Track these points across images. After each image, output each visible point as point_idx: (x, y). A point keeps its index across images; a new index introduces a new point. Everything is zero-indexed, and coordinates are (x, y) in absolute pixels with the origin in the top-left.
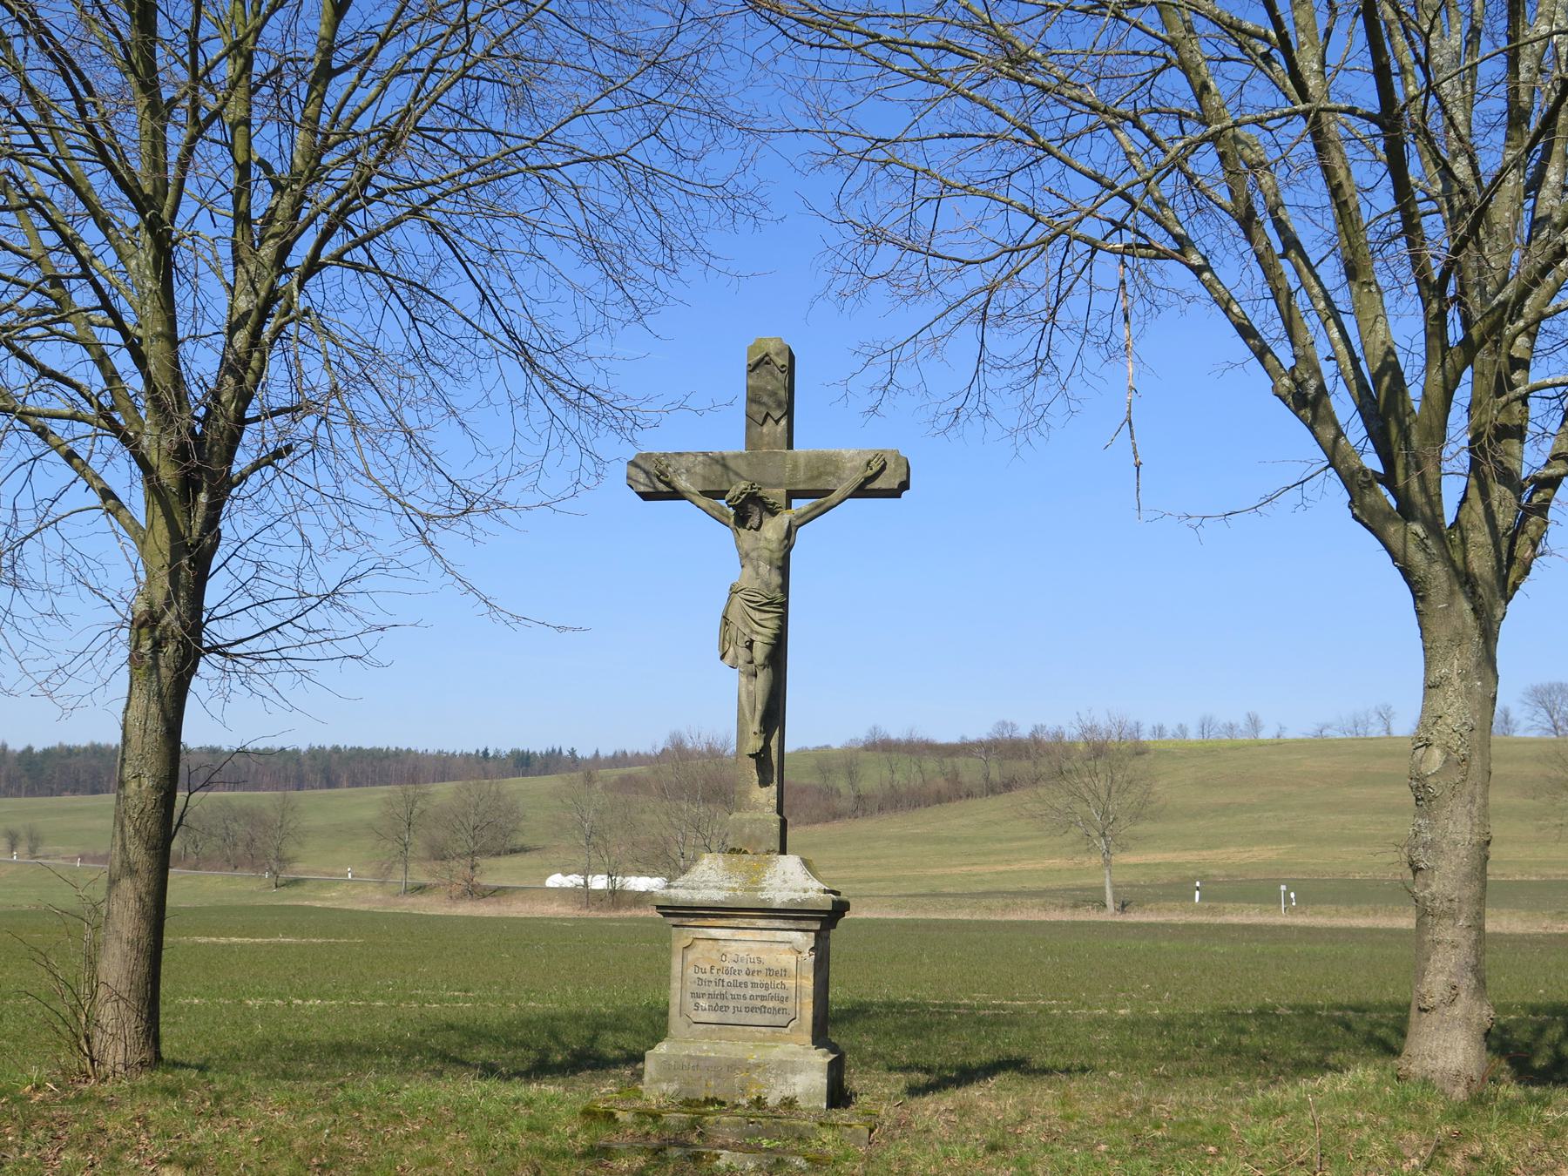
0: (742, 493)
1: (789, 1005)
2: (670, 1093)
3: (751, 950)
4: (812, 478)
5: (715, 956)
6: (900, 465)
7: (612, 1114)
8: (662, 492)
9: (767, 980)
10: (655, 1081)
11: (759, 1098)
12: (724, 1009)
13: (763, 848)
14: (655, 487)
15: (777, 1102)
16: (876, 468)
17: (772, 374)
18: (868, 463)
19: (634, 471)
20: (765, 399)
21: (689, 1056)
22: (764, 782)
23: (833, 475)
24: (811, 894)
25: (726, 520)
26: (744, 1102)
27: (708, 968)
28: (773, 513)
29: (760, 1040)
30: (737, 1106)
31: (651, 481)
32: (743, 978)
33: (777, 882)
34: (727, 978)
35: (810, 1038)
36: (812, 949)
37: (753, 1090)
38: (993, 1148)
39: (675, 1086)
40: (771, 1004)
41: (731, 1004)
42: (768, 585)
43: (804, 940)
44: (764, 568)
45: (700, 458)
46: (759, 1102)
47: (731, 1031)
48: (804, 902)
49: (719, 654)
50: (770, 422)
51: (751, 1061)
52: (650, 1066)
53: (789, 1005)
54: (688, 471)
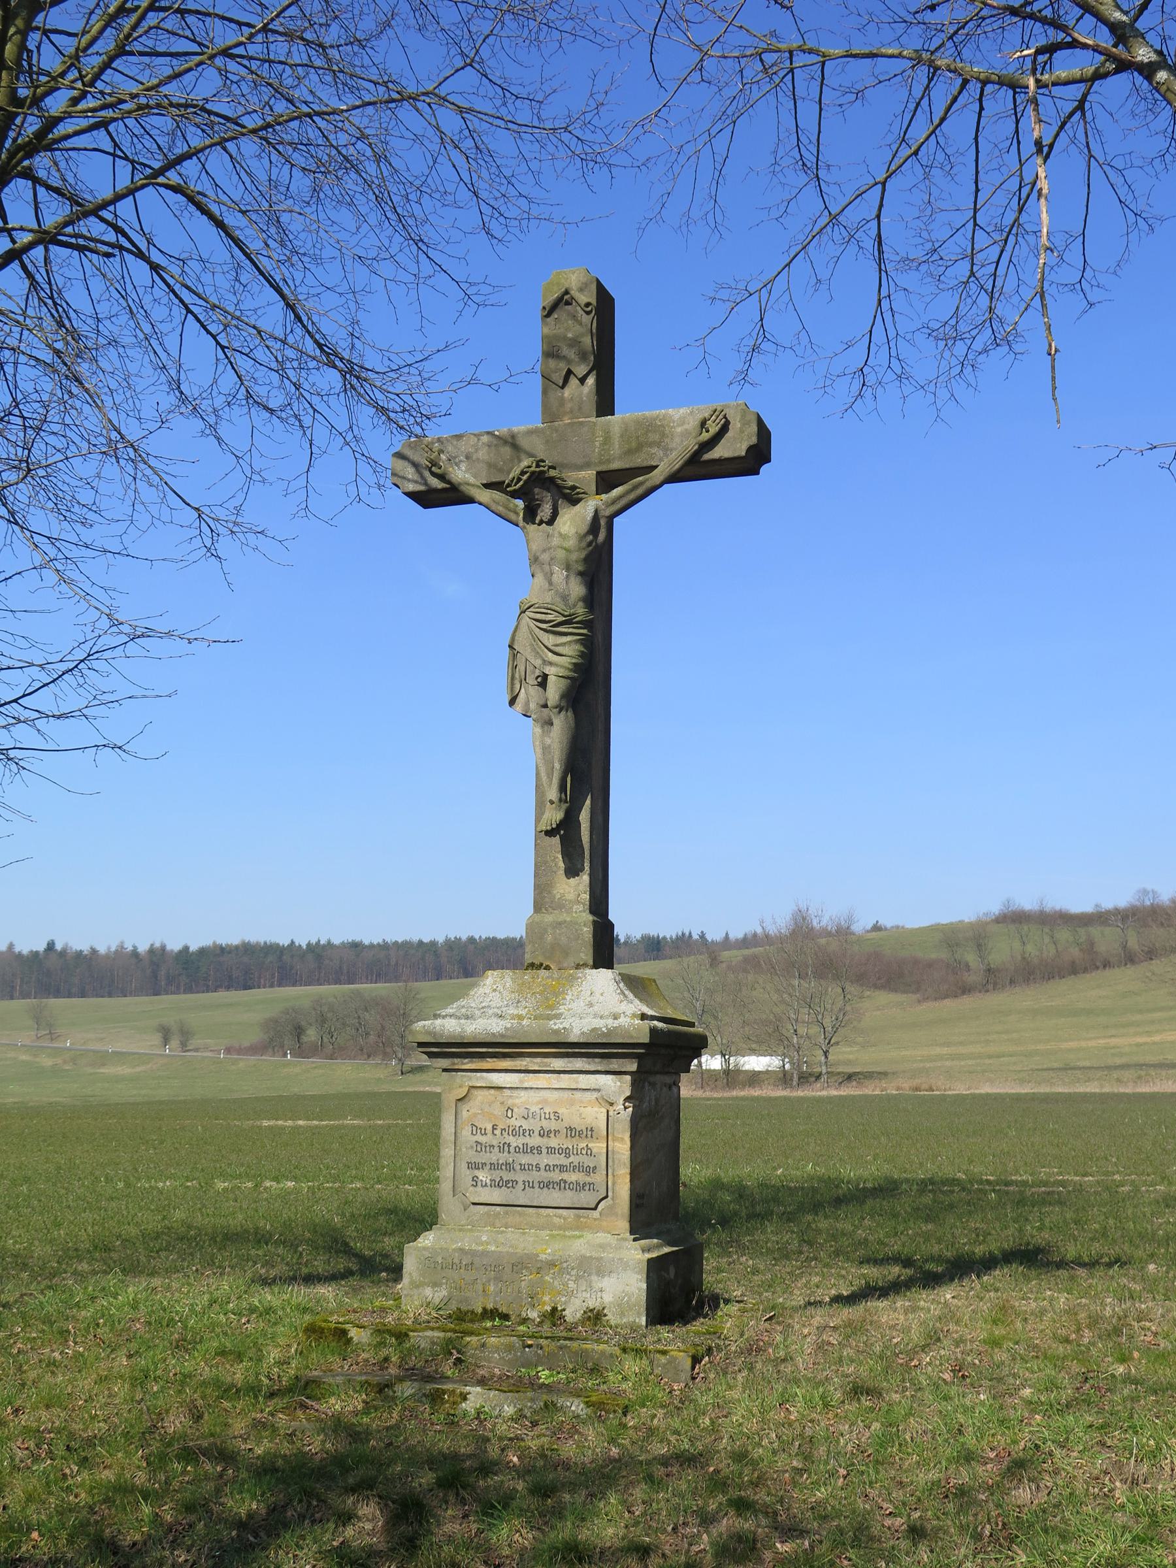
0: (523, 473)
1: (598, 1178)
2: (437, 1301)
3: (545, 1101)
4: (629, 452)
5: (498, 1111)
6: (748, 423)
7: (344, 1332)
8: (436, 490)
9: (568, 1144)
10: (416, 1285)
11: (554, 1309)
12: (510, 1184)
13: (571, 961)
14: (426, 484)
15: (579, 1315)
16: (714, 429)
17: (574, 317)
18: (703, 423)
19: (400, 465)
20: (565, 351)
21: (461, 1250)
22: (572, 871)
23: (658, 444)
24: (623, 1021)
25: (513, 517)
26: (533, 1314)
27: (489, 1127)
28: (574, 501)
29: (560, 1228)
30: (525, 1321)
31: (422, 476)
32: (535, 1141)
33: (579, 1006)
34: (515, 1142)
35: (627, 1225)
36: (627, 1099)
37: (546, 1298)
38: (857, 1391)
39: (443, 1293)
40: (573, 1177)
41: (521, 1177)
42: (565, 598)
43: (617, 1087)
44: (559, 575)
45: (485, 439)
46: (554, 1316)
47: (520, 1214)
48: (610, 1032)
49: (507, 698)
50: (573, 382)
51: (543, 1257)
52: (410, 1265)
53: (598, 1178)
54: (467, 457)
